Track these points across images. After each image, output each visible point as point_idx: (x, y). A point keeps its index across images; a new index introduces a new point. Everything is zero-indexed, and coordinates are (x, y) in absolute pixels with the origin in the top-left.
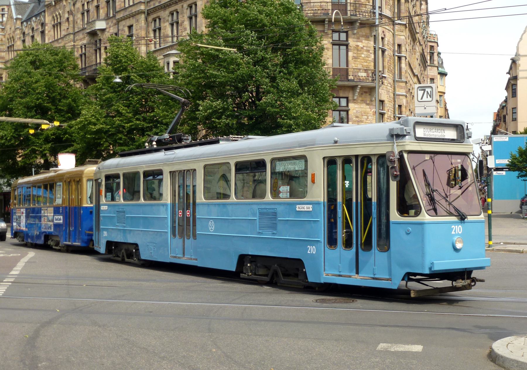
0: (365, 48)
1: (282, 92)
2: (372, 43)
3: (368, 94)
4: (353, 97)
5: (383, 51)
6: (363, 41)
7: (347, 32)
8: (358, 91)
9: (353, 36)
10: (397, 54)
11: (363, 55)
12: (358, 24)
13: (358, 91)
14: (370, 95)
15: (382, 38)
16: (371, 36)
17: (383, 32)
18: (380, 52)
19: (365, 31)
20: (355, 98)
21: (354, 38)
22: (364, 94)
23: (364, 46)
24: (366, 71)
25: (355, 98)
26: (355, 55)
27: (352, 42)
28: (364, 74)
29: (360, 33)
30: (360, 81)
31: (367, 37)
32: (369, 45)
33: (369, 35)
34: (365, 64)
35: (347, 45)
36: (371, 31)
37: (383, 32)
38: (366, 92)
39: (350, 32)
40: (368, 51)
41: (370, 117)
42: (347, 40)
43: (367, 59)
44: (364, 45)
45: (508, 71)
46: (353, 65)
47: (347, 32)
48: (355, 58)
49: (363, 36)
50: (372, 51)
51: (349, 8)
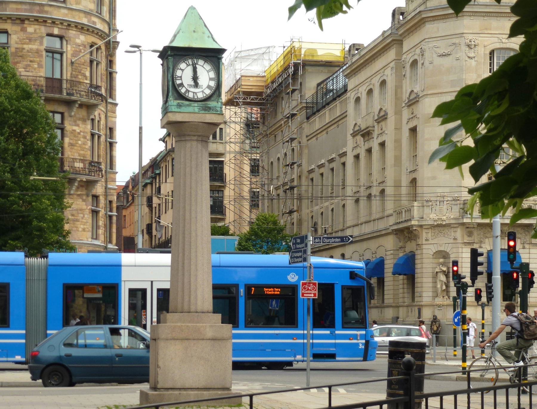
0: (82, 134)
1: (27, 189)
2: (89, 127)
3: (84, 189)
4: (69, 191)
5: (99, 137)
6: (80, 125)
7: (62, 114)
8: (76, 184)
9: (70, 119)
10: (109, 140)
11: (80, 142)
12: (77, 106)
13: (76, 184)
14: (86, 189)
15: (98, 121)
16: (89, 120)
17: (99, 114)
18: (97, 136)
19: (83, 113)
20: (72, 192)
21: (70, 121)
22: (81, 188)
23: (81, 131)
24: (82, 161)
25: (72, 192)
26: (71, 142)
27: (68, 126)
28: (81, 165)
29: (77, 116)
30: (77, 173)
31: (84, 121)
32: (86, 130)
33: (86, 118)
34: (82, 152)
35: (62, 130)
36: (89, 114)
37: (99, 114)
38: (82, 186)
39: (66, 114)
40: (85, 137)
41: (86, 216)
42: (62, 123)
43: (84, 146)
44: (81, 129)
45: (162, 137)
46: (70, 153)
47: (62, 114)
48: (71, 145)
49: (80, 119)
50: (89, 137)
51: (64, 86)
